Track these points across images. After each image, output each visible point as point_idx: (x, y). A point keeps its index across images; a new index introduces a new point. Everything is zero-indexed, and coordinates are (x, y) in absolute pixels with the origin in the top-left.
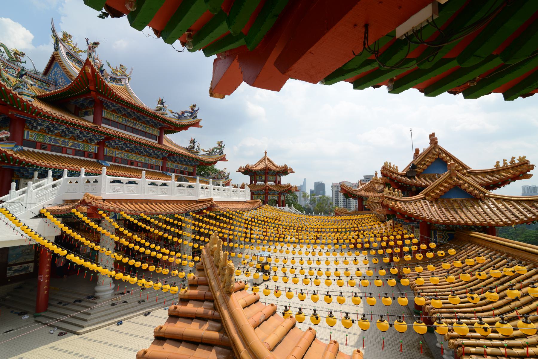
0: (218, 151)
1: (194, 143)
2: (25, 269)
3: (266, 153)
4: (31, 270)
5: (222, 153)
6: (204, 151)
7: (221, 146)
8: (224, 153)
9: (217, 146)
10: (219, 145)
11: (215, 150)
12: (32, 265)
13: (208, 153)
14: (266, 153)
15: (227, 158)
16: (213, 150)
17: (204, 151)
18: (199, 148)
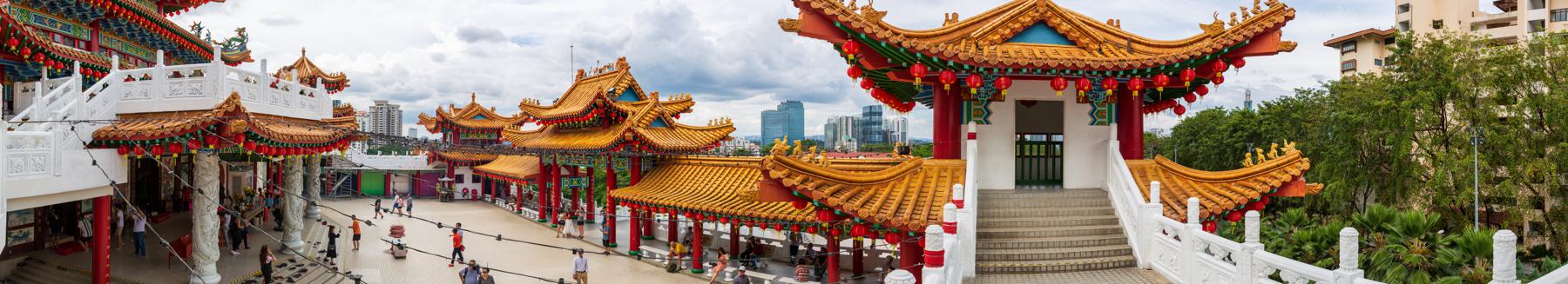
2: (26, 235)
4: (32, 237)
12: (32, 229)
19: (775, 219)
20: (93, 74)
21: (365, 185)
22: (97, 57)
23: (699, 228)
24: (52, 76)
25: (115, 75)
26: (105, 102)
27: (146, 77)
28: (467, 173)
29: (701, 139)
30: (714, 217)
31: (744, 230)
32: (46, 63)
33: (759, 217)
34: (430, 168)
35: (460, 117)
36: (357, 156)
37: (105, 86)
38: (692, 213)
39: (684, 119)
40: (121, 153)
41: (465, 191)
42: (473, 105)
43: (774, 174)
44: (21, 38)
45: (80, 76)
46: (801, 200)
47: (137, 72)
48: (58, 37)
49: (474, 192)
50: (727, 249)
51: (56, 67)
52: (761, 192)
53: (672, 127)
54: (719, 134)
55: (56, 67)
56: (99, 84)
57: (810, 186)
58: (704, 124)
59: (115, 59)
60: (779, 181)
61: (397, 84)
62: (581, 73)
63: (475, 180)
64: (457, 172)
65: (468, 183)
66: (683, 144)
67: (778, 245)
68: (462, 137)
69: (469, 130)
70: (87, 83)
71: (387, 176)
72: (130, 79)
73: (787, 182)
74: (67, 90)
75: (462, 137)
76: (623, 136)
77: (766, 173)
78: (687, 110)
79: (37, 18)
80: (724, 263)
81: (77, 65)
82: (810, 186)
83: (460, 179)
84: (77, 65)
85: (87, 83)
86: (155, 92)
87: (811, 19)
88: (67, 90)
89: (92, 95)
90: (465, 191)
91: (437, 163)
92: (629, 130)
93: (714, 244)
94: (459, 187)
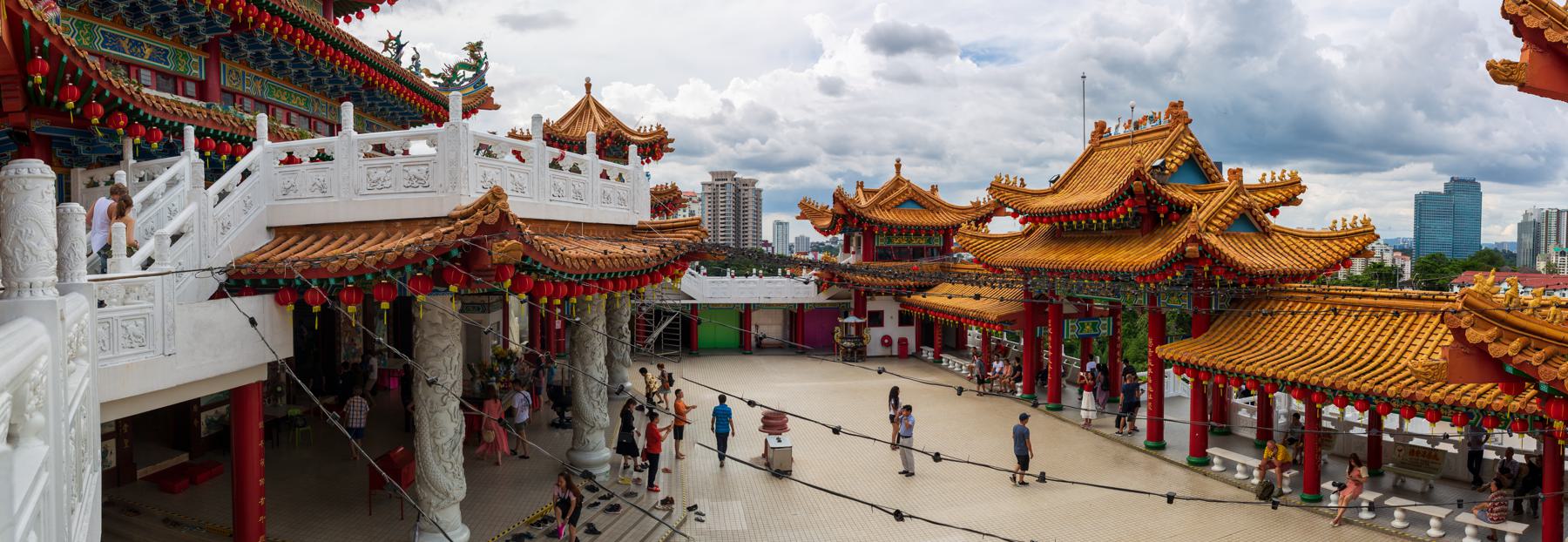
0: (469, 74)
1: (400, 47)
3: (588, 86)
5: (483, 82)
6: (429, 75)
7: (477, 59)
8: (490, 79)
9: (465, 56)
10: (473, 56)
11: (461, 72)
13: (440, 80)
14: (588, 86)
15: (497, 98)
16: (454, 71)
17: (429, 75)
18: (417, 66)
19: (1455, 405)
20: (222, 152)
21: (706, 332)
22: (227, 114)
23: (1314, 416)
24: (143, 154)
25: (263, 151)
26: (247, 206)
27: (322, 157)
28: (889, 309)
29: (1318, 255)
30: (1344, 398)
31: (1391, 421)
32: (130, 132)
33: (1426, 401)
34: (822, 298)
35: (875, 205)
36: (699, 287)
37: (246, 174)
38: (1303, 390)
39: (1286, 218)
40: (281, 302)
41: (886, 341)
42: (898, 182)
43: (1474, 336)
44: (84, 83)
45: (195, 155)
46: (1515, 381)
47: (305, 146)
48: (146, 75)
49: (903, 342)
50: (1363, 454)
51: (148, 139)
52: (1449, 366)
53: (1265, 232)
54: (1349, 245)
55: (148, 139)
56: (234, 173)
57: (1535, 358)
58: (1320, 227)
59: (262, 120)
60: (1481, 348)
61: (753, 142)
62: (1101, 128)
63: (904, 320)
64: (872, 306)
65: (891, 327)
66: (1287, 263)
67: (1450, 448)
68: (880, 242)
69: (891, 229)
70: (214, 172)
71: (745, 313)
72: (291, 159)
73: (1496, 350)
74: (172, 183)
75: (880, 242)
76: (1182, 250)
77: (1459, 333)
78: (1292, 201)
79: (110, 40)
80: (1358, 483)
81: (190, 132)
82: (1535, 358)
83: (877, 319)
84: (190, 132)
85: (214, 172)
86: (350, 182)
87: (1543, 61)
88: (172, 183)
89: (223, 195)
90: (886, 341)
91: (835, 290)
92: (1193, 239)
93: (1338, 445)
94: (875, 334)
